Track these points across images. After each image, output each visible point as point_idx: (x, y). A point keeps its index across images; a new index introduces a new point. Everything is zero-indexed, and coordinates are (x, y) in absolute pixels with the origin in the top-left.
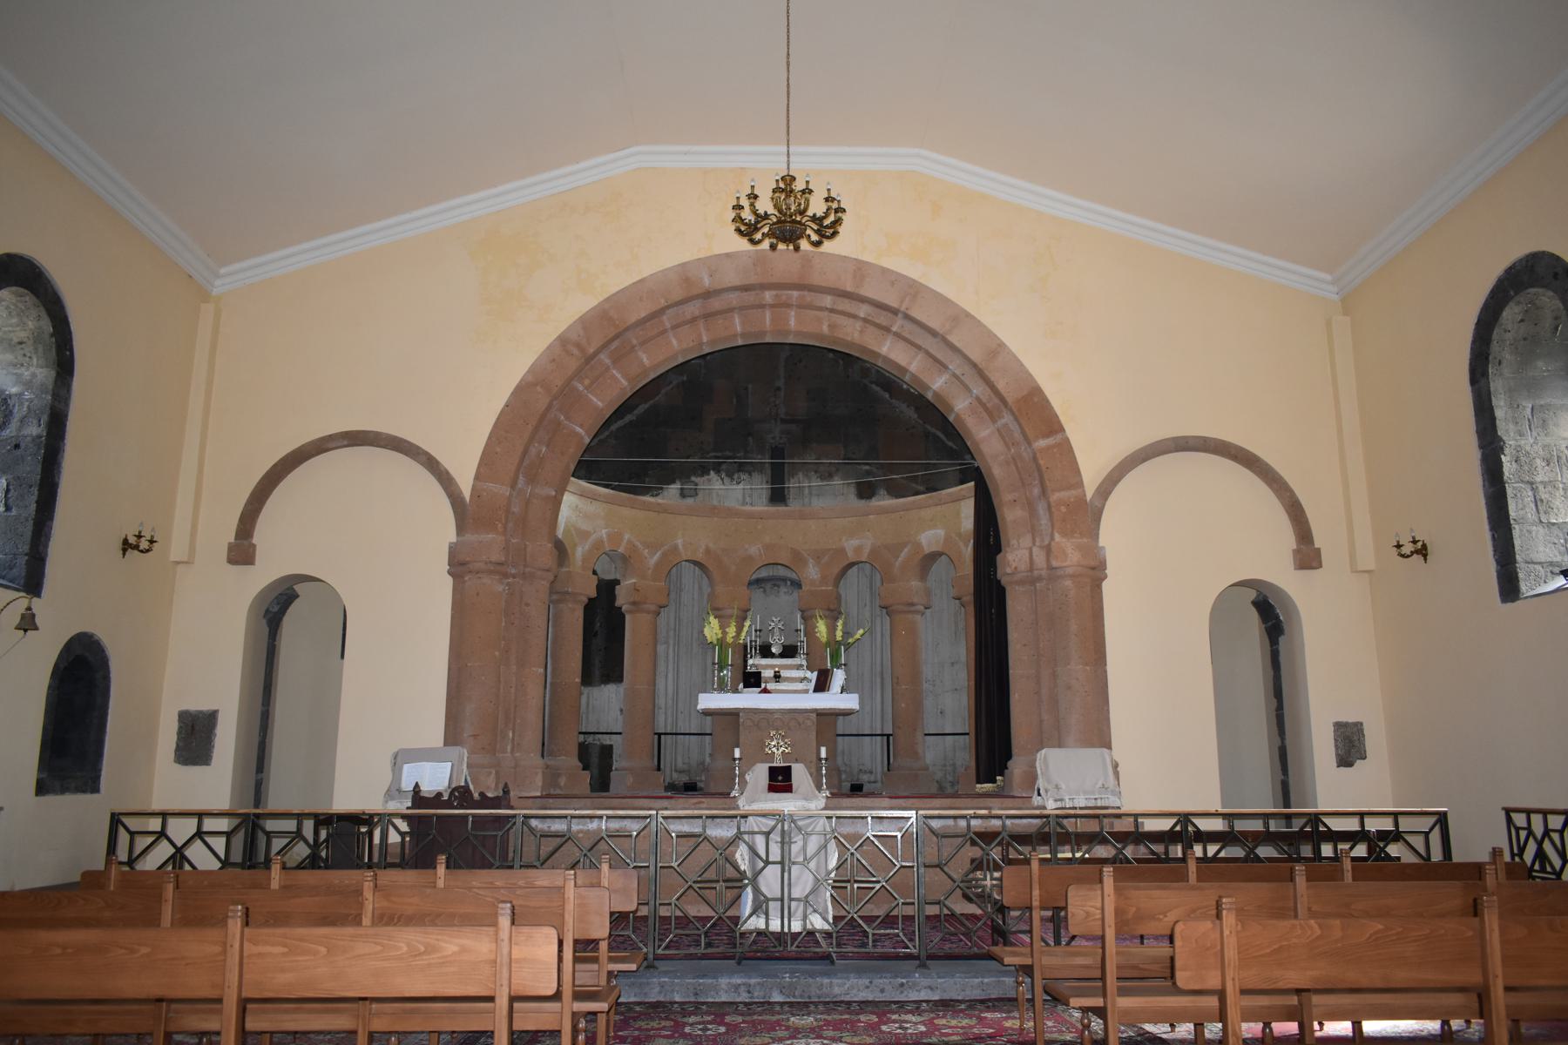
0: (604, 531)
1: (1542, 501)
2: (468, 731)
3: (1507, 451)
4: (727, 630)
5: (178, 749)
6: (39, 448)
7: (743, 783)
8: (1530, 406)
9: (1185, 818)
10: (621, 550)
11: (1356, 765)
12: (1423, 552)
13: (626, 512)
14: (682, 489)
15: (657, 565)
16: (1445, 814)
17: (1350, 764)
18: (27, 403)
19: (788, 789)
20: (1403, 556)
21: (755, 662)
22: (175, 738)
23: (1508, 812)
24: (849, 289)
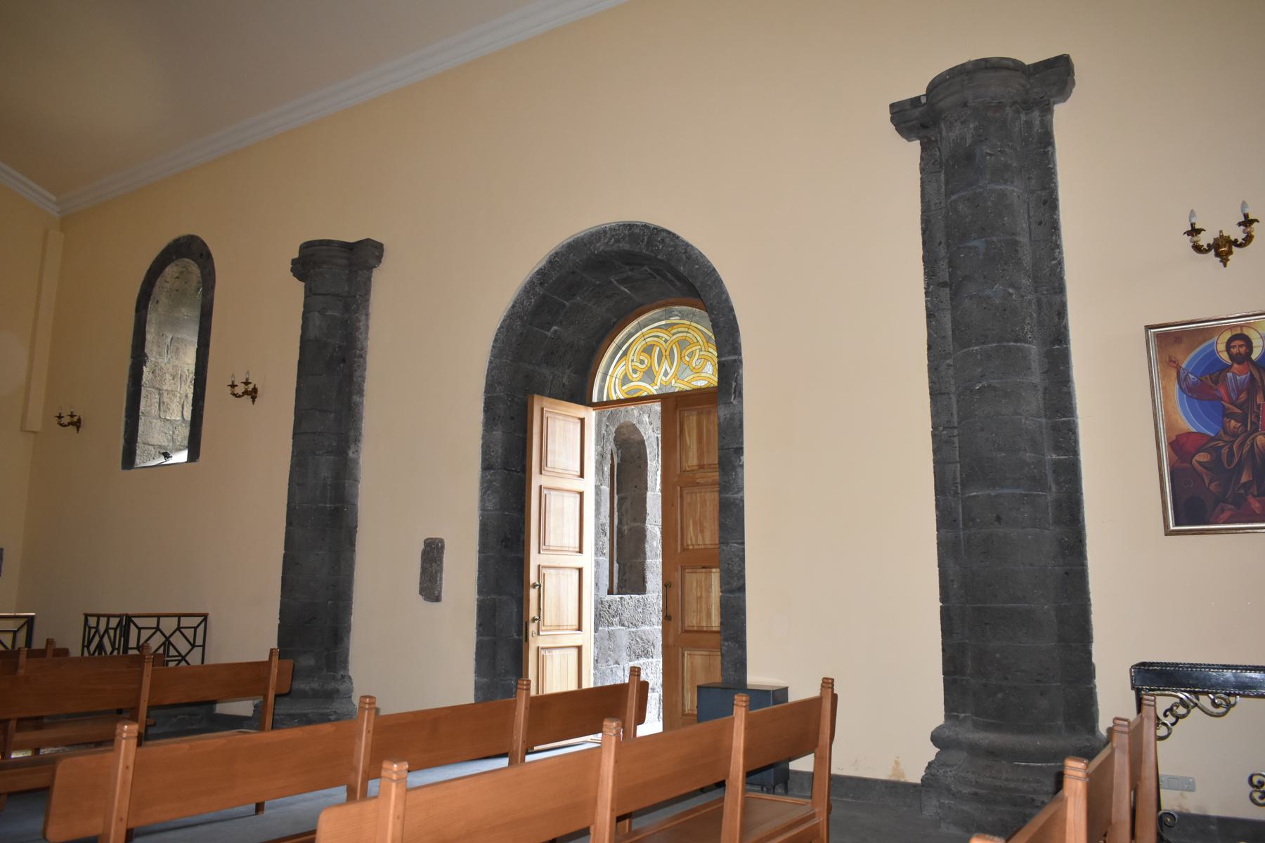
1: (164, 403)
3: (148, 364)
8: (171, 337)
12: (77, 424)
16: (32, 617)
20: (61, 425)
23: (87, 616)
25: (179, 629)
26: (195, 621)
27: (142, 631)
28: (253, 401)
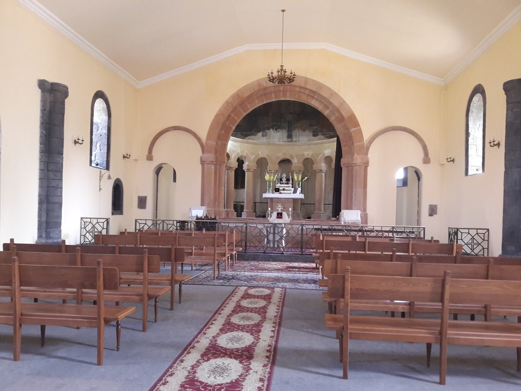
0: (240, 150)
1: (478, 150)
2: (206, 202)
3: (470, 136)
4: (271, 177)
5: (138, 205)
6: (106, 136)
7: (271, 217)
9: (393, 228)
10: (244, 155)
11: (434, 216)
12: (453, 161)
13: (245, 145)
14: (263, 134)
15: (254, 158)
17: (432, 216)
18: (102, 125)
19: (281, 218)
20: (448, 161)
21: (278, 185)
22: (137, 202)
24: (303, 85)
25: (477, 234)
26: (484, 231)
27: (463, 233)
28: (499, 148)
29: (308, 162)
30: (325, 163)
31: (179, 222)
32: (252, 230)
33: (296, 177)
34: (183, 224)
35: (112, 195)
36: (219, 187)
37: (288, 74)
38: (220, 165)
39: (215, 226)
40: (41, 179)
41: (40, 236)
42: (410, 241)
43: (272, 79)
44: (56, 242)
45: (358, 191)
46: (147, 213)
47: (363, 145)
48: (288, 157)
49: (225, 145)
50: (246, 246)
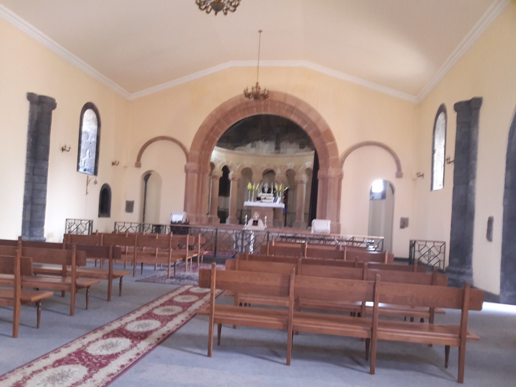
2: (188, 209)
12: (423, 175)
15: (239, 169)
21: (260, 194)
24: (282, 101)
29: (290, 174)
30: (306, 173)
31: (155, 226)
32: (221, 235)
33: (276, 187)
34: (158, 228)
35: (99, 199)
36: (201, 194)
37: (261, 91)
38: (203, 174)
39: (188, 231)
40: (27, 182)
41: (23, 233)
42: (344, 249)
43: (247, 95)
44: (38, 240)
45: (331, 202)
46: (135, 217)
47: (337, 159)
48: (272, 168)
49: (209, 155)
50: (215, 250)
